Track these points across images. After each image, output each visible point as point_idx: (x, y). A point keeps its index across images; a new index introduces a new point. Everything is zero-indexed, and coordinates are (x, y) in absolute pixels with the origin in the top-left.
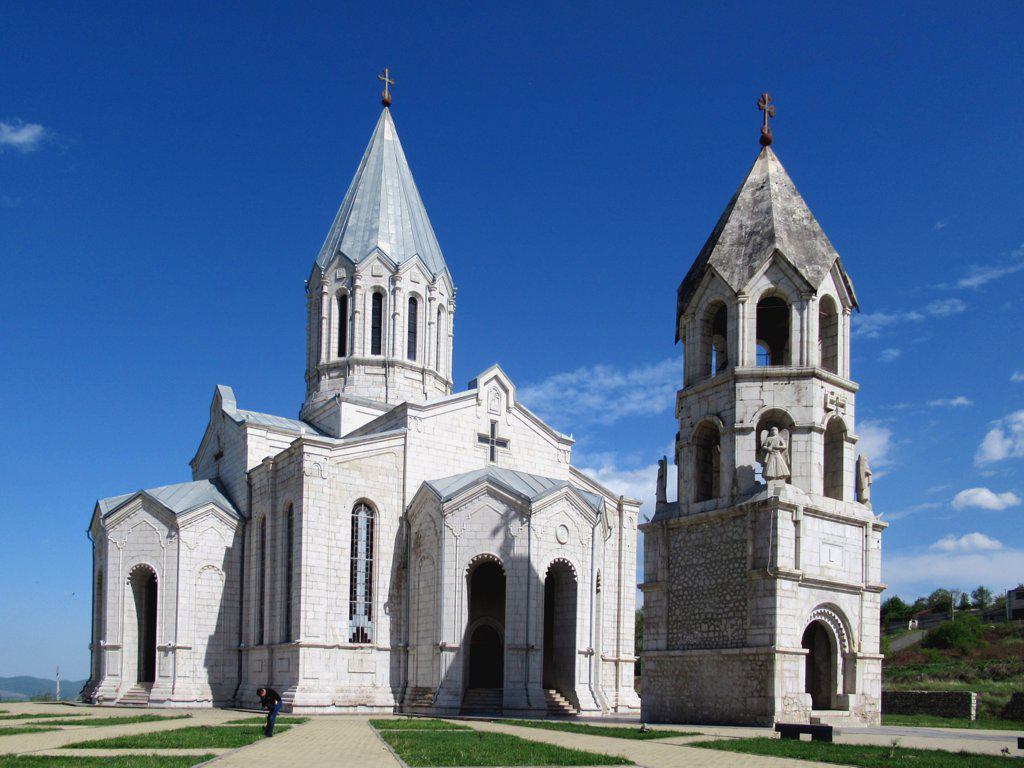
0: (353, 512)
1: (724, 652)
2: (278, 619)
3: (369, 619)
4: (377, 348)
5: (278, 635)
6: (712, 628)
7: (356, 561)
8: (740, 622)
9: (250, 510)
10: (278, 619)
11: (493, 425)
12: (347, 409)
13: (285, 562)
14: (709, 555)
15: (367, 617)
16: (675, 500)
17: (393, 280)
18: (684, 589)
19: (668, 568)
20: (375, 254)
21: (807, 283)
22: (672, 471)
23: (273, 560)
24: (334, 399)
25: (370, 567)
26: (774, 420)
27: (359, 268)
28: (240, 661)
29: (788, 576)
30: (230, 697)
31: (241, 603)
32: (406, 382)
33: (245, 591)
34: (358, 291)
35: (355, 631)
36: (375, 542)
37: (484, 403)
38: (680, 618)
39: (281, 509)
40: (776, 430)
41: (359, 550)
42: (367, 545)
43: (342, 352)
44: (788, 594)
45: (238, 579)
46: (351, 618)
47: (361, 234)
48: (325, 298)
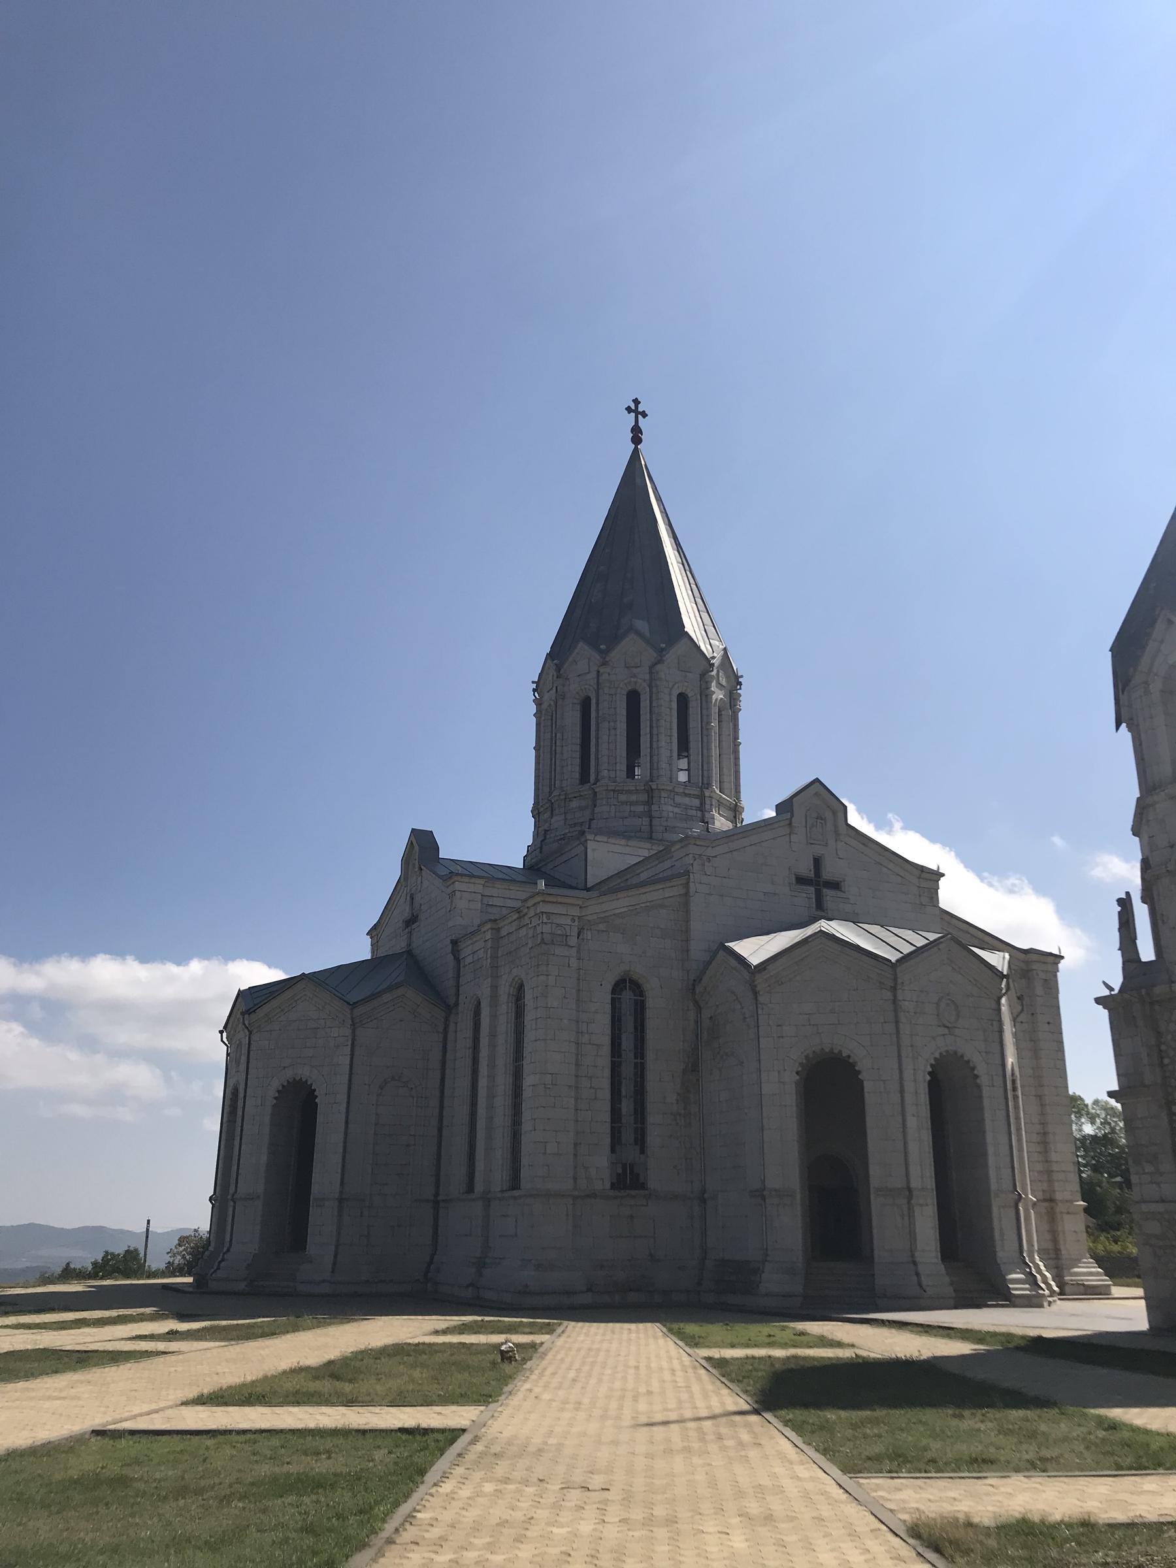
0: (613, 992)
5: (499, 1177)
7: (620, 1063)
9: (457, 995)
11: (817, 862)
16: (1153, 958)
19: (1162, 1065)
20: (632, 636)
22: (1141, 914)
23: (492, 1065)
28: (436, 1219)
31: (440, 1130)
32: (677, 810)
34: (606, 690)
35: (620, 1171)
39: (505, 990)
41: (624, 1047)
43: (584, 778)
46: (613, 1150)
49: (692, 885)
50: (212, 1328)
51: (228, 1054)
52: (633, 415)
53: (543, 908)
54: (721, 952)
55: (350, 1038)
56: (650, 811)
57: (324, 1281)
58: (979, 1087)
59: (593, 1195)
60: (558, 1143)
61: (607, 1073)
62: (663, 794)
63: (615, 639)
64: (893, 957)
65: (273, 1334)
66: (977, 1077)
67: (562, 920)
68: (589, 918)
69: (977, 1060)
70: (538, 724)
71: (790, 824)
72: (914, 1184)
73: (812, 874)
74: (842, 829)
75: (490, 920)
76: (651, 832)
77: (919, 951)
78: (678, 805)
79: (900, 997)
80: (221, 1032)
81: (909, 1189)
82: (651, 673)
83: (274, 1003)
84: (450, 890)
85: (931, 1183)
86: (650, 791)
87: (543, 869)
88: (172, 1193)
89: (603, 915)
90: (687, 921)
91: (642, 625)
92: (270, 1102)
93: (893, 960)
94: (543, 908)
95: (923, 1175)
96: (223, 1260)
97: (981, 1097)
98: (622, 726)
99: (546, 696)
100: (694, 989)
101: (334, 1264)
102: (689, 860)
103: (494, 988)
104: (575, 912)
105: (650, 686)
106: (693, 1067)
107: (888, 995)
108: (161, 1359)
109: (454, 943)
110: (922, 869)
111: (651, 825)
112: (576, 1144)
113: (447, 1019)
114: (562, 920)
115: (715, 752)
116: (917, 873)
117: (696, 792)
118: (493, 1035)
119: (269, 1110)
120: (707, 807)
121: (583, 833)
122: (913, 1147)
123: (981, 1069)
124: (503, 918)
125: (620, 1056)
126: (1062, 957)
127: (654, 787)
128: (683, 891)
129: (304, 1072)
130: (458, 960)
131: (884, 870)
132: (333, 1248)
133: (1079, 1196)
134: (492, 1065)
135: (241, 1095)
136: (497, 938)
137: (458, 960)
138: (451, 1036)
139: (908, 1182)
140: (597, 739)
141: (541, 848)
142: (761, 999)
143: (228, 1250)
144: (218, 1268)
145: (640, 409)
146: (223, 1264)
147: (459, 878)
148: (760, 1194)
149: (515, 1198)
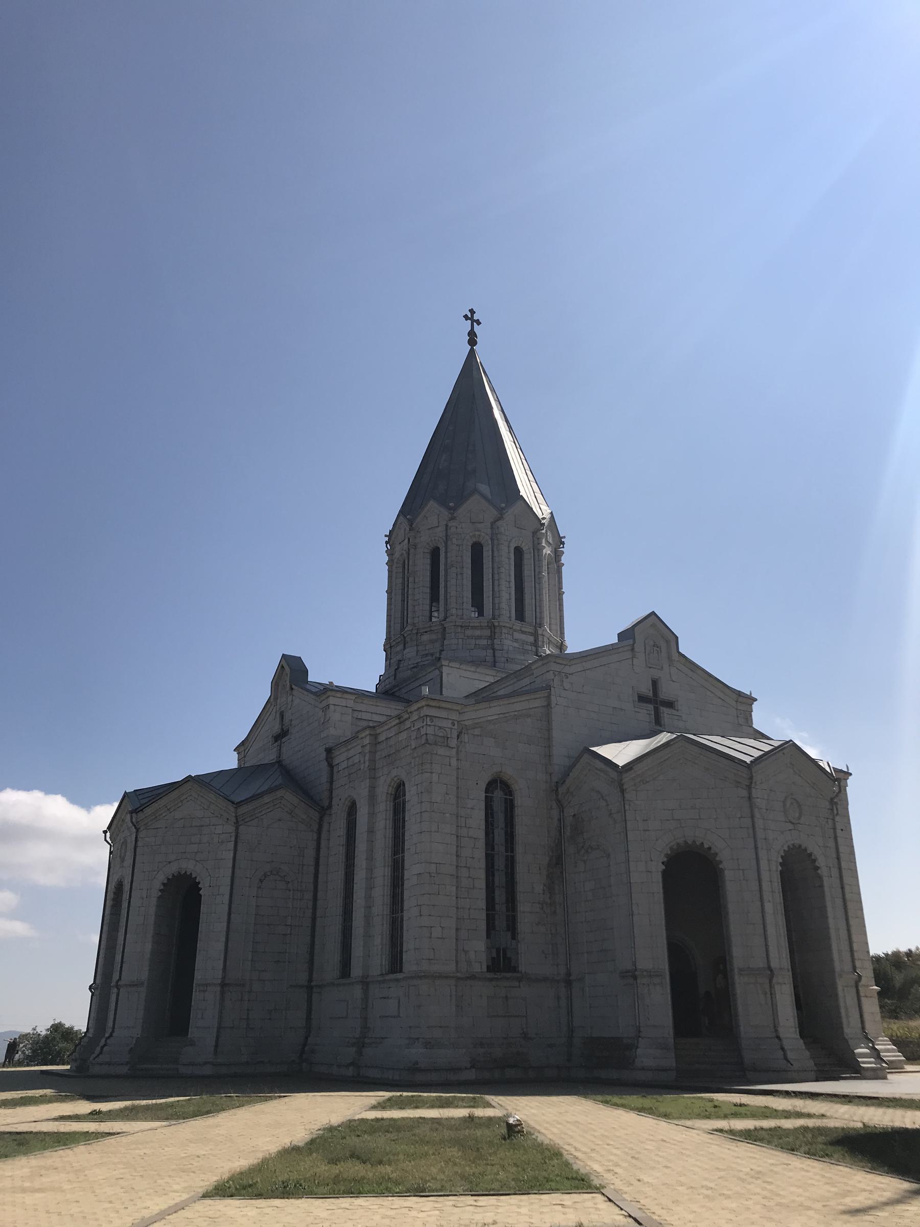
2: (378, 941)
3: (514, 938)
5: (378, 962)
9: (331, 798)
10: (378, 941)
11: (655, 683)
15: (509, 934)
23: (370, 858)
25: (511, 863)
31: (314, 919)
32: (516, 645)
33: (319, 903)
34: (454, 541)
35: (494, 955)
39: (384, 789)
42: (506, 833)
45: (311, 887)
49: (553, 698)
50: (133, 1109)
51: (111, 853)
52: (469, 321)
53: (426, 711)
54: (586, 756)
55: (234, 834)
56: (493, 644)
57: (206, 1063)
58: (820, 878)
59: (473, 977)
60: (442, 928)
61: (483, 864)
62: (504, 631)
63: (462, 498)
64: (748, 760)
65: (208, 1113)
66: (818, 868)
68: (467, 723)
69: (817, 852)
70: (390, 571)
71: (633, 649)
72: (773, 965)
73: (651, 694)
74: (675, 656)
75: (370, 727)
76: (495, 662)
77: (767, 753)
78: (516, 640)
79: (754, 796)
80: (105, 832)
81: (770, 968)
82: (492, 528)
83: (162, 802)
84: (324, 704)
85: (786, 963)
86: (492, 627)
87: (397, 694)
88: (51, 983)
89: (477, 721)
90: (549, 730)
91: (484, 488)
92: (155, 894)
93: (748, 762)
94: (426, 711)
95: (780, 958)
96: (105, 1045)
97: (822, 886)
98: (468, 572)
99: (398, 548)
100: (557, 789)
101: (216, 1046)
102: (550, 675)
103: (372, 788)
104: (454, 716)
105: (492, 540)
106: (557, 861)
107: (744, 793)
108: (111, 1140)
109: (329, 751)
110: (739, 694)
111: (494, 656)
112: (457, 929)
113: (321, 819)
115: (546, 598)
116: (735, 696)
117: (531, 630)
118: (371, 831)
119: (154, 901)
120: (540, 643)
121: (439, 659)
122: (771, 931)
123: (821, 862)
124: (381, 724)
125: (493, 849)
126: (851, 774)
127: (496, 624)
128: (545, 704)
129: (188, 866)
130: (331, 766)
131: (709, 693)
132: (215, 1030)
133: (874, 983)
134: (370, 858)
135: (127, 887)
136: (375, 743)
137: (331, 766)
138: (324, 835)
139: (768, 961)
140: (446, 581)
141: (395, 675)
142: (626, 795)
143: (111, 1035)
144: (101, 1053)
145: (475, 318)
146: (105, 1048)
147: (333, 693)
148: (631, 975)
149: (397, 980)
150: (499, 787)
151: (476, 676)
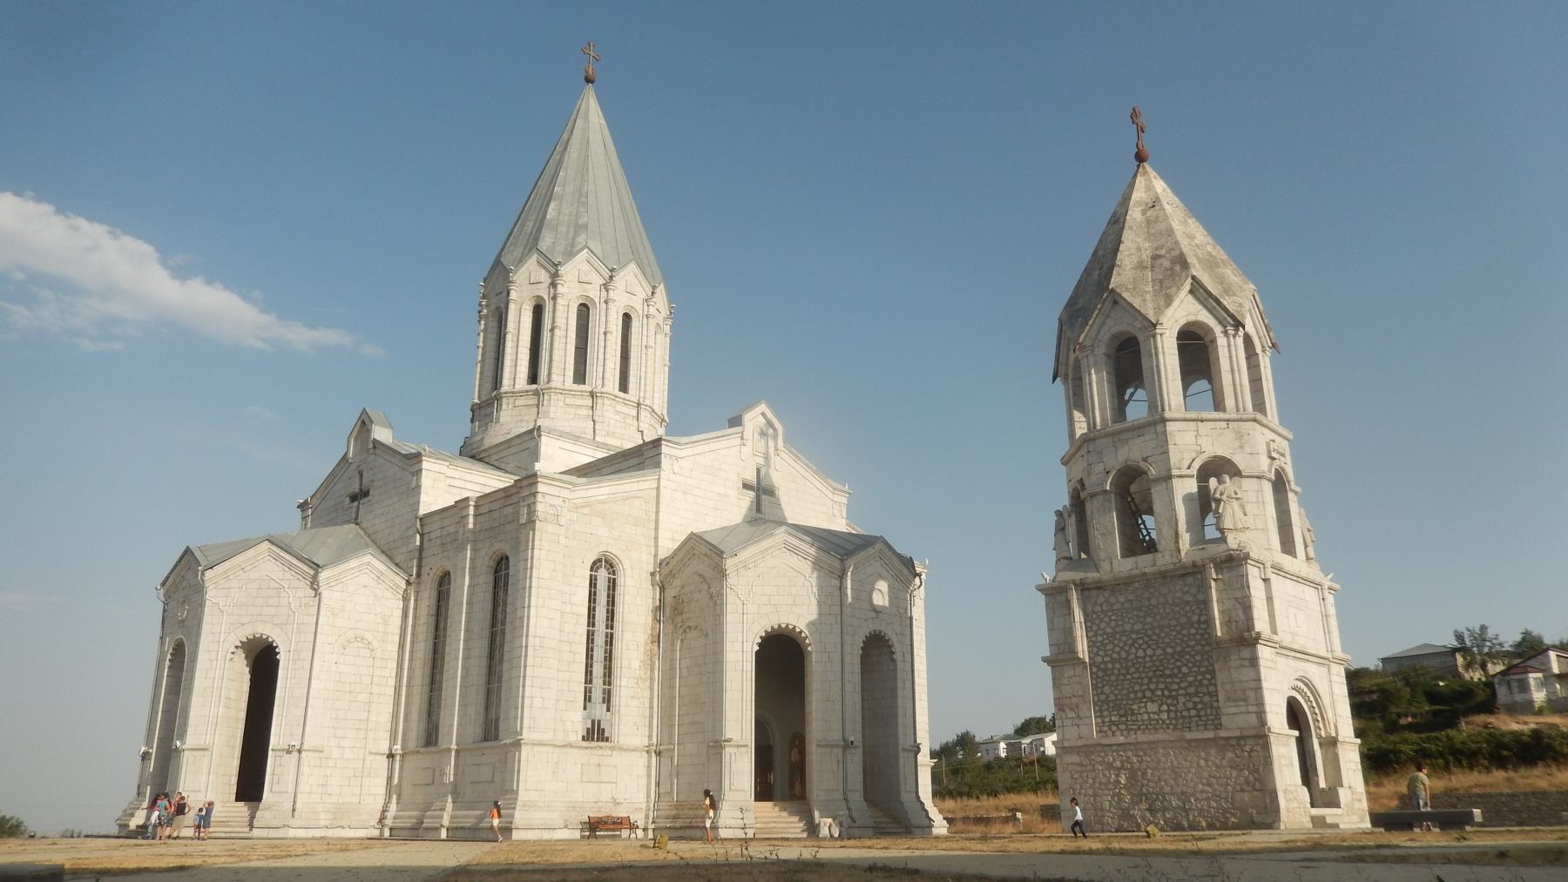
1: (1189, 736)
4: (580, 376)
6: (1165, 707)
8: (1206, 699)
12: (547, 445)
13: (487, 633)
14: (1149, 620)
17: (606, 287)
18: (1113, 661)
21: (1232, 316)
24: (531, 431)
25: (610, 640)
26: (1216, 468)
27: (562, 270)
29: (1271, 643)
30: (374, 822)
34: (560, 301)
36: (618, 609)
37: (749, 444)
38: (1112, 697)
40: (1227, 477)
43: (533, 378)
44: (1270, 664)
47: (564, 229)
48: (512, 307)
58: (894, 661)
59: (570, 746)
63: (570, 254)
67: (558, 502)
97: (895, 670)
104: (565, 493)
107: (837, 583)
114: (558, 502)
150: (605, 564)
151: (575, 448)
